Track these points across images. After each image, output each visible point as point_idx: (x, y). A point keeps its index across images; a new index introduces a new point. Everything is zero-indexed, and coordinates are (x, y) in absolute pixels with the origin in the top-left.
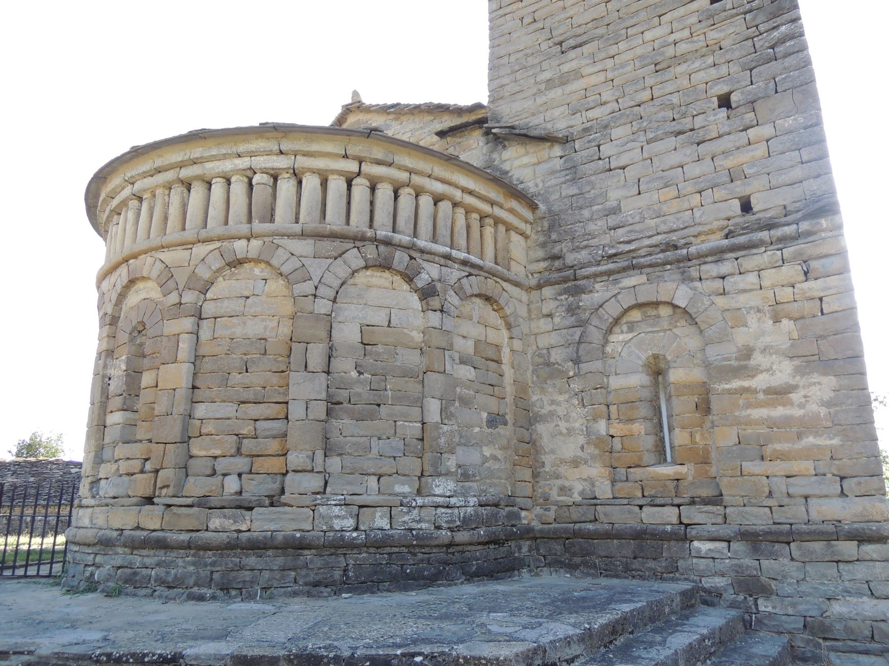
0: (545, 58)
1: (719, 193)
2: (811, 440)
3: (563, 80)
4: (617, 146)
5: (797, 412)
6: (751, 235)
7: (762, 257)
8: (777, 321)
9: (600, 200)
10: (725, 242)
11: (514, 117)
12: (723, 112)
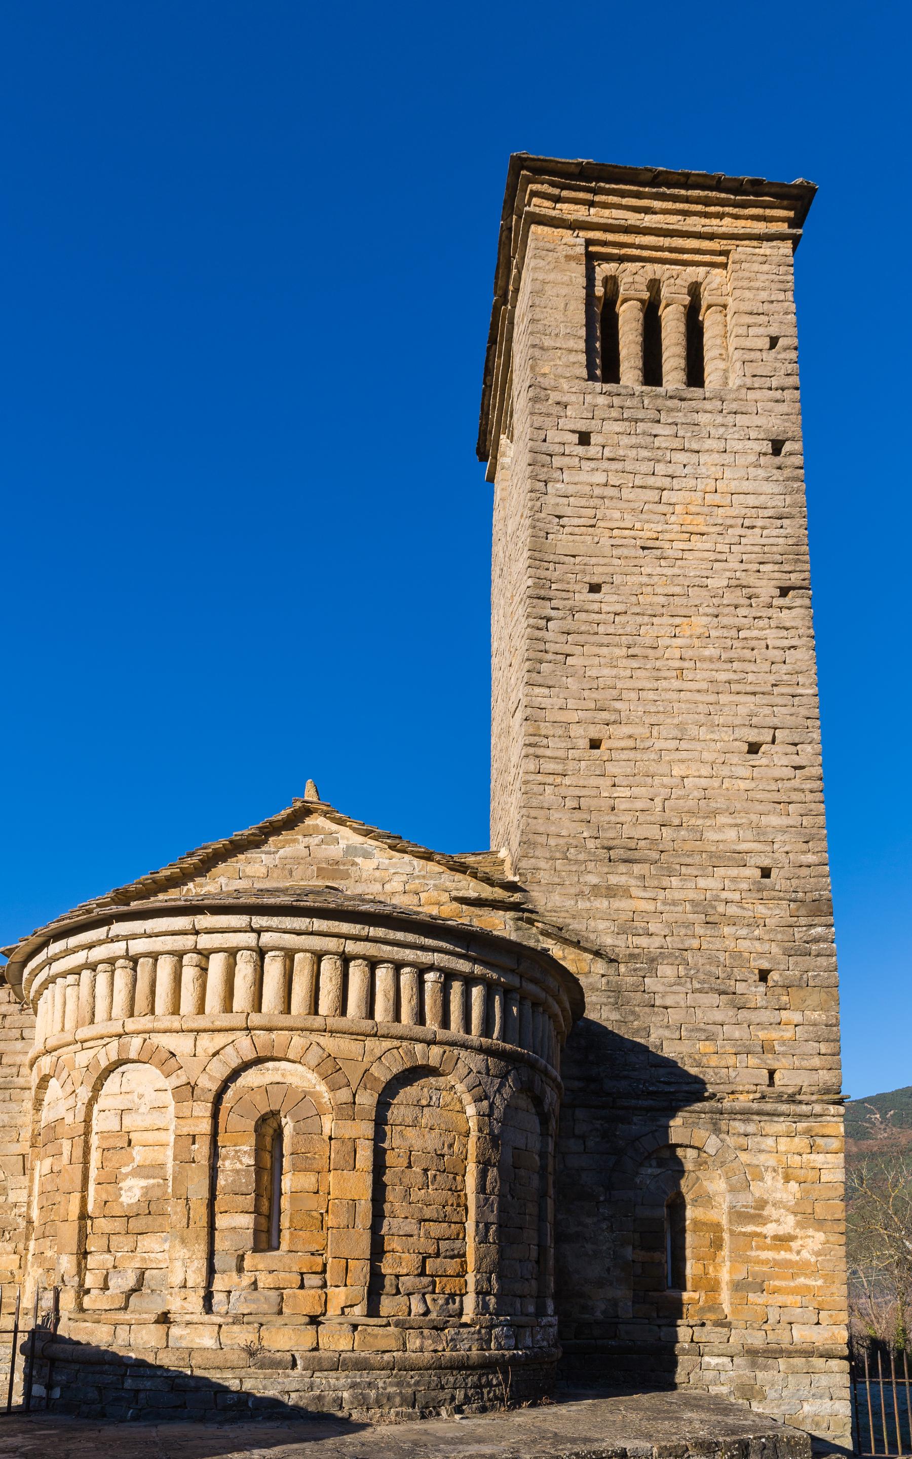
0: (592, 858)
1: (753, 1061)
2: (802, 1280)
3: (611, 892)
4: (663, 984)
5: (794, 1257)
6: (777, 1105)
7: (780, 1126)
8: (787, 1180)
9: (644, 1034)
10: (755, 1106)
11: (550, 911)
12: (762, 988)
